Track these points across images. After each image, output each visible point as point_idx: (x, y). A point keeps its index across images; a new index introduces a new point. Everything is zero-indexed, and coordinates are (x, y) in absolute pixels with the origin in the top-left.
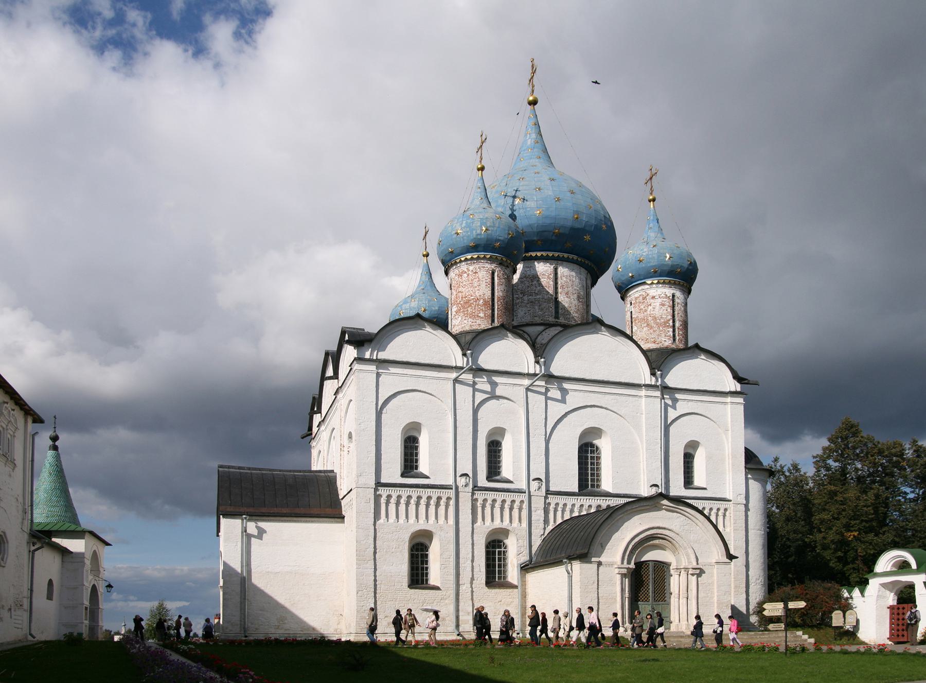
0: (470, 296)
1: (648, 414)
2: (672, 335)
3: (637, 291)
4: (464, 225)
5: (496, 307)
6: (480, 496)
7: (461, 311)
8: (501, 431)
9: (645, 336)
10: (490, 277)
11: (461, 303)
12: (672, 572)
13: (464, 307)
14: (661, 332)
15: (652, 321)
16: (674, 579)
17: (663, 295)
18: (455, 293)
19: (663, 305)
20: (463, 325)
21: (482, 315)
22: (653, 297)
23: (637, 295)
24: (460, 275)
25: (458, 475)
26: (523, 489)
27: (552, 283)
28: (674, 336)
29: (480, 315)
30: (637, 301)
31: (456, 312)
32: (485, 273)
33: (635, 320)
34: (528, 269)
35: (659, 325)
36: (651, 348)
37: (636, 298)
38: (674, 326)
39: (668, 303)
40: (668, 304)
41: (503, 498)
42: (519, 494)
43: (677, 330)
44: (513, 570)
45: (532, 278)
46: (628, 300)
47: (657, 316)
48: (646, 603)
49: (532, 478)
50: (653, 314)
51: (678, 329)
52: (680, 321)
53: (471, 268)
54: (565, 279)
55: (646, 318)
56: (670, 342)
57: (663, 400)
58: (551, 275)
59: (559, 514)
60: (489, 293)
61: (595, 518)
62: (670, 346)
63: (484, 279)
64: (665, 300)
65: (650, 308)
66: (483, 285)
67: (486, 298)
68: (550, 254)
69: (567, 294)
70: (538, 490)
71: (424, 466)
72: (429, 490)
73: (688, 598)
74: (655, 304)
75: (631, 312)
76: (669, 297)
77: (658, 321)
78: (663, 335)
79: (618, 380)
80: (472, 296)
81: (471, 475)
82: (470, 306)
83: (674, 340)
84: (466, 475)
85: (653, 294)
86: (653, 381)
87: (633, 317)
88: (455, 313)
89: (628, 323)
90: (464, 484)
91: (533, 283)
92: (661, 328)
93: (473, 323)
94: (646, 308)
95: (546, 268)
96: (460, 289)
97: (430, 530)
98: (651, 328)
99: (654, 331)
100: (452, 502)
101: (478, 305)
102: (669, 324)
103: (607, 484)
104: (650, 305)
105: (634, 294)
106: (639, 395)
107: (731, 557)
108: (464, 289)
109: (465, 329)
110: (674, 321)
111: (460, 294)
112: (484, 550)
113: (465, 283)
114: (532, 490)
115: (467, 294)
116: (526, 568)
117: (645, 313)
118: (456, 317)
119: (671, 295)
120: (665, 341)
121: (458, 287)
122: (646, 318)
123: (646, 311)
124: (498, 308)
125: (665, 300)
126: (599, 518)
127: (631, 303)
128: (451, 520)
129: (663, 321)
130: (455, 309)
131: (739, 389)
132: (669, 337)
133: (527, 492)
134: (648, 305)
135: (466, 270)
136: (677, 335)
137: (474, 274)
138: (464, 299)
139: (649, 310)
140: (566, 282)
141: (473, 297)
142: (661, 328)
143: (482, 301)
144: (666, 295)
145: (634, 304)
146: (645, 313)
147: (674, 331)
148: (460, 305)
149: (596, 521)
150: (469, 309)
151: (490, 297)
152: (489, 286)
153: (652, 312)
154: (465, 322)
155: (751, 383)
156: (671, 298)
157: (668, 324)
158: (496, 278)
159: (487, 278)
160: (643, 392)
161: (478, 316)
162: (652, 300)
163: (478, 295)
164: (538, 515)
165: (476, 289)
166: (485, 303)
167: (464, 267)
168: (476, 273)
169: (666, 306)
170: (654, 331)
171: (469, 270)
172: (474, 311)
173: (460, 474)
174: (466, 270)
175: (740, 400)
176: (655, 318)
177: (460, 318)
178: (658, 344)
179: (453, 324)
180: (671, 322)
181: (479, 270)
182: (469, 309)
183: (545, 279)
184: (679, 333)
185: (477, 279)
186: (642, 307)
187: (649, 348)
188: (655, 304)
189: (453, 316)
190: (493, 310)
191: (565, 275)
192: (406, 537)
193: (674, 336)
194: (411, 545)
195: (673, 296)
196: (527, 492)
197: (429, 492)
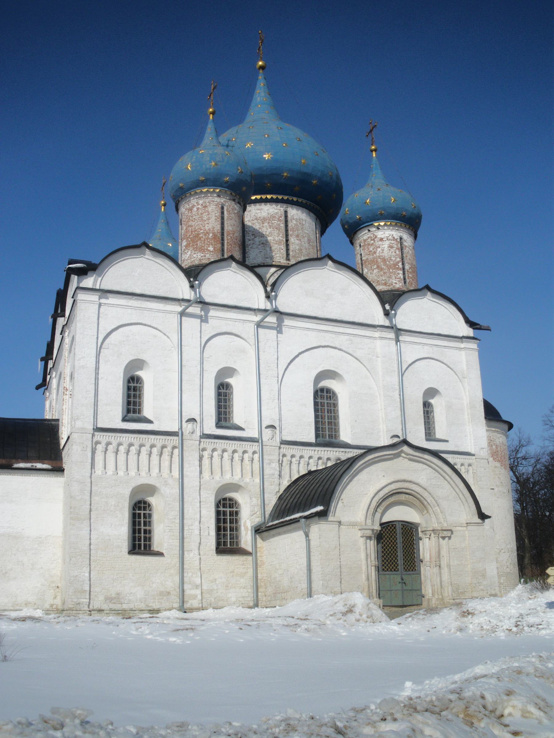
0: (199, 230)
1: (383, 357)
2: (402, 277)
3: (365, 234)
4: (194, 160)
5: (226, 242)
6: (209, 444)
7: (191, 245)
8: (228, 371)
9: (376, 278)
10: (219, 211)
11: (191, 236)
12: (421, 535)
13: (193, 241)
14: (391, 274)
15: (382, 263)
16: (423, 544)
17: (390, 237)
18: (185, 228)
19: (392, 247)
20: (193, 259)
21: (211, 248)
22: (381, 240)
23: (365, 237)
24: (190, 210)
25: (184, 420)
26: (256, 438)
27: (283, 226)
28: (405, 279)
29: (209, 249)
30: (366, 243)
31: (186, 246)
32: (215, 206)
33: (365, 262)
34: (259, 211)
35: (389, 267)
36: (383, 290)
37: (365, 241)
38: (404, 269)
39: (396, 245)
40: (396, 246)
41: (233, 448)
42: (251, 443)
43: (406, 272)
44: (246, 534)
45: (263, 220)
46: (357, 243)
47: (386, 258)
48: (395, 573)
49: (264, 425)
50: (382, 256)
51: (408, 271)
52: (409, 264)
53: (201, 202)
54: (295, 222)
55: (375, 260)
56: (401, 285)
57: (398, 343)
58: (281, 217)
59: (294, 467)
60: (218, 227)
61: (334, 470)
62: (401, 288)
63: (213, 213)
64: (392, 242)
65: (379, 250)
66: (213, 219)
67: (216, 231)
68: (280, 197)
69: (297, 236)
70: (271, 439)
71: (147, 412)
72: (153, 437)
73: (440, 566)
74: (383, 246)
75: (361, 254)
76: (396, 239)
77: (388, 263)
78: (393, 278)
79: (351, 320)
80: (201, 230)
81: (198, 421)
82: (200, 239)
83: (405, 283)
84: (193, 420)
85: (380, 236)
86: (387, 323)
87: (363, 259)
88: (185, 248)
89: (358, 265)
90: (191, 431)
91: (264, 225)
92: (391, 270)
93: (203, 257)
94: (375, 250)
95: (276, 211)
96: (190, 223)
97: (153, 484)
98: (382, 269)
99: (384, 273)
100: (176, 451)
101: (208, 238)
102: (399, 266)
103: (345, 435)
104: (379, 247)
105: (363, 236)
106: (374, 336)
107: (483, 516)
108: (193, 223)
109: (194, 264)
110: (403, 264)
111: (190, 228)
112: (214, 509)
113: (194, 217)
114: (264, 439)
115: (197, 228)
116: (259, 530)
117: (375, 255)
118: (186, 251)
119: (398, 238)
120: (396, 283)
121: (188, 221)
122: (375, 260)
123: (375, 253)
124: (227, 243)
125: (392, 242)
126: (339, 469)
127: (360, 245)
128: (176, 473)
129: (392, 263)
130: (184, 243)
131: (472, 335)
132: (398, 280)
133: (260, 441)
134: (377, 247)
135: (196, 204)
136: (407, 278)
137: (204, 208)
138: (194, 233)
139: (378, 252)
140: (296, 225)
141: (202, 231)
142: (391, 270)
143: (211, 235)
144: (394, 238)
145: (363, 246)
146: (375, 255)
147: (404, 274)
148: (190, 239)
149: (335, 474)
150: (198, 243)
151: (220, 231)
152: (218, 220)
153: (381, 254)
154: (194, 255)
155: (482, 328)
156: (399, 240)
157: (397, 266)
158: (225, 213)
159: (216, 212)
160: (377, 334)
161: (207, 249)
162: (380, 242)
163: (207, 228)
164: (271, 469)
165: (206, 222)
166: (215, 235)
167: (193, 201)
168: (205, 207)
169: (395, 249)
170: (384, 273)
171: (198, 205)
172: (203, 245)
173: (186, 419)
174: (196, 204)
175: (473, 345)
176: (384, 260)
177: (189, 253)
178: (389, 286)
179: (182, 259)
180: (400, 265)
181: (208, 204)
182: (198, 243)
183: (276, 221)
184: (408, 276)
185: (207, 213)
186: (371, 249)
187: (380, 290)
188: (383, 246)
189: (183, 250)
190: (223, 245)
191: (295, 218)
192: (127, 492)
193: (405, 279)
194: (133, 502)
195: (401, 239)
196: (260, 441)
197: (152, 438)
